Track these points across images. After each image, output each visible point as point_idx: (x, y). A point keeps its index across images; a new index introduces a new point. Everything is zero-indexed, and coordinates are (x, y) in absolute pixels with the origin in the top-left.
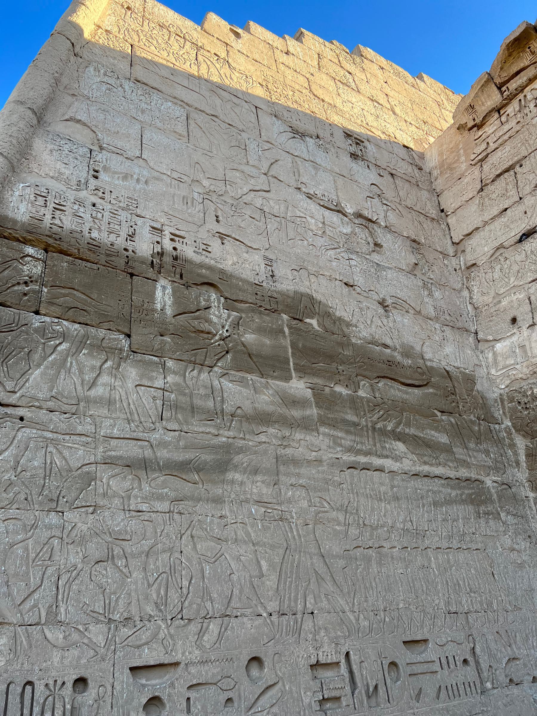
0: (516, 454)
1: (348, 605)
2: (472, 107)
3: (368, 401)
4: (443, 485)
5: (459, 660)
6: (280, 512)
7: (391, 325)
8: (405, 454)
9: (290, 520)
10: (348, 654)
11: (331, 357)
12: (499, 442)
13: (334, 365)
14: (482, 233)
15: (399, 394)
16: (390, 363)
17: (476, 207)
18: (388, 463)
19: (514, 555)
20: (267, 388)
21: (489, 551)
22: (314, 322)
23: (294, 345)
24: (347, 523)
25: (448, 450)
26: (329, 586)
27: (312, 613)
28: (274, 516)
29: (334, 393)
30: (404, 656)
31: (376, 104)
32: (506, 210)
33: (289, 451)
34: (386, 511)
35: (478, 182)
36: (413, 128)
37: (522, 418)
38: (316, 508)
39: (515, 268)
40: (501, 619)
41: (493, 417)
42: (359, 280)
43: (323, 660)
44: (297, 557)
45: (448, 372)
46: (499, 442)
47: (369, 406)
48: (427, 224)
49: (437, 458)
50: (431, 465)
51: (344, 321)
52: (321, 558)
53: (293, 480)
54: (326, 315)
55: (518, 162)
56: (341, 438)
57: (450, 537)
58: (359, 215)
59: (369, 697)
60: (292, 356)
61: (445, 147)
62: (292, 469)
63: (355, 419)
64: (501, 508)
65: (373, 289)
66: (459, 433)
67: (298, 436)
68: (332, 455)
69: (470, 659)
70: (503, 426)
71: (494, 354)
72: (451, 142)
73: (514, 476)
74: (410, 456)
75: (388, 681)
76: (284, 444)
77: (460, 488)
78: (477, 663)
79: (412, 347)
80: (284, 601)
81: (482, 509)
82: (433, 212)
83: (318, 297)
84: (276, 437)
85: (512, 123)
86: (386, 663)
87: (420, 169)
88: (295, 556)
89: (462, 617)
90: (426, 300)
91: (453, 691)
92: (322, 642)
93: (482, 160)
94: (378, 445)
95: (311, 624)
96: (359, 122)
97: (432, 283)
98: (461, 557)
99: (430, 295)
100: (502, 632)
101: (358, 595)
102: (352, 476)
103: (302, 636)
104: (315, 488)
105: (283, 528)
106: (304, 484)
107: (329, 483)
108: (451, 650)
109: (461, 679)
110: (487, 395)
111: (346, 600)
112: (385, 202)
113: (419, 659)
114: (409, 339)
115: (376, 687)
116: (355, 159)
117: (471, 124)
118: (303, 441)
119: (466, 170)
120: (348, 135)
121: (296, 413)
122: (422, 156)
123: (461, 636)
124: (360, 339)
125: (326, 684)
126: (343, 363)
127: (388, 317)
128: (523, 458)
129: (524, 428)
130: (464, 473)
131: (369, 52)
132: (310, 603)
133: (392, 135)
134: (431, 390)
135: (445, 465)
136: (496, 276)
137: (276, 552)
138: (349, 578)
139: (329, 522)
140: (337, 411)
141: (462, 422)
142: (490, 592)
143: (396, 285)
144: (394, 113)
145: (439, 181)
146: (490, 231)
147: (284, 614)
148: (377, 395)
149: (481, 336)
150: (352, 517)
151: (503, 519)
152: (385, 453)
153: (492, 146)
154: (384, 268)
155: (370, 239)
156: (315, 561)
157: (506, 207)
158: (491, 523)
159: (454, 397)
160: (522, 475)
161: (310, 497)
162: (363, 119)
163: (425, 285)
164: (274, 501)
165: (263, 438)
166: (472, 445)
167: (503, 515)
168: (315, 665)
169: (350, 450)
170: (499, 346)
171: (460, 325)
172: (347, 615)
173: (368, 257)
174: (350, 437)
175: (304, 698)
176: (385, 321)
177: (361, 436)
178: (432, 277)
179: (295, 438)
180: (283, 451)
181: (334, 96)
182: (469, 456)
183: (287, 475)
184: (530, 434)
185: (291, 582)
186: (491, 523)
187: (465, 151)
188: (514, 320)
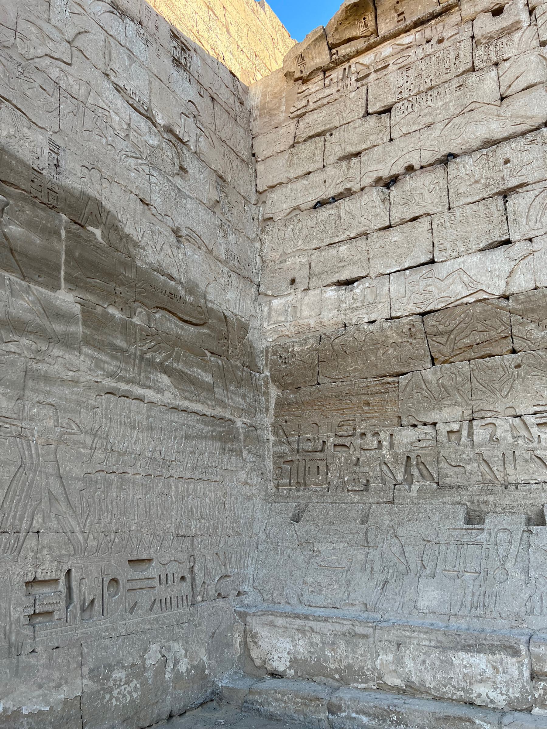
0: (267, 401)
1: (79, 526)
2: (302, 57)
3: (142, 329)
4: (197, 421)
5: (178, 576)
6: (20, 429)
7: (181, 257)
8: (168, 387)
9: (30, 438)
10: (69, 571)
11: (109, 275)
12: (256, 389)
13: (112, 285)
14: (284, 190)
15: (174, 328)
16: (172, 295)
17: (285, 161)
18: (149, 394)
19: (245, 489)
20: (28, 293)
21: (226, 483)
22: (98, 232)
23: (69, 252)
24: (94, 446)
25: (210, 389)
26: (63, 507)
27: (38, 532)
28: (11, 432)
29: (106, 315)
30: (126, 574)
31: (211, 13)
32: (310, 173)
33: (41, 367)
34: (137, 439)
35: (292, 137)
36: (243, 57)
37: (279, 371)
38: (62, 429)
39: (305, 232)
40: (222, 543)
41: (256, 365)
42: (157, 200)
43: (40, 577)
44: (31, 475)
46: (256, 389)
47: (141, 334)
48: (236, 164)
49: (198, 395)
50: (191, 401)
51: (132, 240)
52: (59, 480)
53: (41, 398)
54: (113, 228)
55: (330, 130)
56: (105, 362)
57: (194, 469)
58: (170, 131)
59: (83, 610)
60: (65, 264)
61: (269, 89)
62: (42, 385)
63: (124, 345)
64: (245, 446)
65: (169, 214)
66: (224, 375)
67: (56, 352)
68: (91, 378)
69: (188, 576)
70: (263, 375)
72: (276, 86)
73: (261, 420)
74: (173, 390)
75: (106, 596)
76: (38, 358)
77: (212, 425)
78: (193, 579)
79: (197, 285)
80: (7, 519)
81: (228, 446)
82: (245, 154)
83: (109, 206)
84: (29, 349)
85: (333, 90)
86: (107, 579)
87: (242, 103)
88: (29, 474)
89: (188, 540)
90: (220, 241)
91: (165, 604)
92: (43, 560)
93: (300, 116)
94: (143, 375)
95: (34, 542)
96: (189, 25)
97: (229, 226)
98: (200, 487)
99: (225, 237)
100: (221, 554)
101: (91, 517)
102: (109, 401)
103: (21, 554)
104: (65, 409)
105: (20, 445)
106: (53, 403)
107: (83, 405)
108: (172, 568)
109: (176, 593)
110: (255, 345)
111: (78, 521)
112: (199, 125)
113: (140, 576)
114: (196, 276)
115: (92, 602)
117: (297, 75)
118: (60, 359)
119: (284, 121)
120: (175, 36)
121: (58, 328)
122: (246, 91)
123: (183, 556)
124: (146, 264)
125: (39, 600)
126: (122, 284)
127: (179, 248)
128: (272, 405)
130: (219, 412)
132: (38, 522)
133: (221, 55)
134: (206, 331)
135: (204, 403)
136: (287, 236)
137: (6, 470)
138: (85, 500)
139: (75, 444)
140: (105, 333)
141: (228, 366)
142: (218, 519)
143: (193, 217)
144: (228, 32)
145: (257, 123)
146: (292, 189)
147: (4, 532)
148: (152, 325)
150: (100, 442)
151: (244, 456)
152: (148, 383)
153: (312, 106)
154: (185, 196)
155: (176, 160)
156: (51, 481)
157: (310, 170)
158: (233, 459)
159: (226, 341)
160: (268, 420)
161: (58, 417)
162: (195, 24)
163: (222, 225)
164: (15, 416)
165: (12, 347)
166: (232, 388)
167: (244, 453)
168: (32, 582)
169: (112, 375)
170: (275, 302)
171: (246, 274)
172: (76, 535)
173: (170, 178)
174: (115, 363)
175: (12, 614)
176: (175, 251)
177: (127, 363)
178: (230, 219)
179: (52, 354)
180: (34, 366)
182: (228, 397)
183: (36, 391)
184: (282, 386)
185: (19, 501)
186: (233, 459)
187: (287, 101)
188: (293, 281)
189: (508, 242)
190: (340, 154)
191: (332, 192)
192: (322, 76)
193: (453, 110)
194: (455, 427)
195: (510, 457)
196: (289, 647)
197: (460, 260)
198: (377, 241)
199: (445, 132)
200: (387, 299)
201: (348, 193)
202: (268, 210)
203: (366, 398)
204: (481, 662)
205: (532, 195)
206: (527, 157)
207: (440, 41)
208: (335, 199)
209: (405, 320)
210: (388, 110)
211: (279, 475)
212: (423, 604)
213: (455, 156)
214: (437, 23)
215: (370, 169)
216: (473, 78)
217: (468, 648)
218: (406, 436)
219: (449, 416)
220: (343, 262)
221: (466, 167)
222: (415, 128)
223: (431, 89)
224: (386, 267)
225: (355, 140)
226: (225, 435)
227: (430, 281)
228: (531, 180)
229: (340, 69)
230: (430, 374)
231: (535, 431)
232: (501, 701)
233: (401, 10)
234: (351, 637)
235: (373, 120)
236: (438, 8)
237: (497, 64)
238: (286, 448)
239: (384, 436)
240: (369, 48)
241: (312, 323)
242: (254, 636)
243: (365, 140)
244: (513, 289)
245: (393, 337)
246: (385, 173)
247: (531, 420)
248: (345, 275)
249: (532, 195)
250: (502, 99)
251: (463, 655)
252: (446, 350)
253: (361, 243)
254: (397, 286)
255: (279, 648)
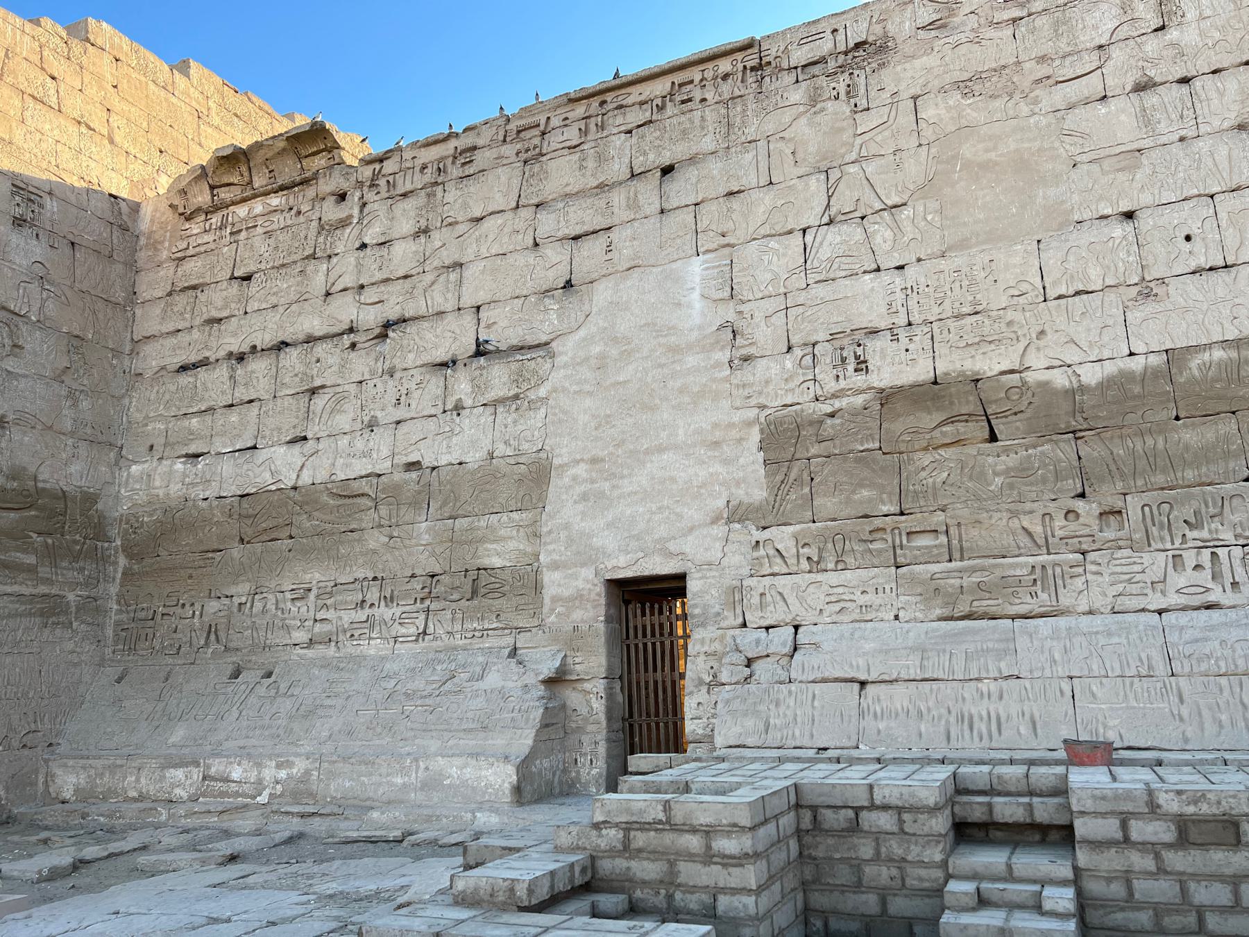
0: (115, 571)
4: (12, 602)
25: (31, 570)
35: (170, 282)
39: (167, 397)
45: (64, 492)
55: (203, 285)
71: (129, 474)
79: (25, 469)
85: (208, 238)
97: (82, 391)
99: (75, 405)
110: (107, 514)
114: (24, 459)
116: (19, 225)
117: (181, 210)
129: (127, 550)
130: (43, 589)
131: (103, 31)
133: (95, 181)
135: (21, 584)
144: (111, 141)
149: (124, 453)
153: (191, 251)
154: (16, 376)
160: (114, 589)
162: (53, 160)
178: (85, 382)
181: (14, 124)
182: (57, 574)
184: (130, 556)
188: (152, 447)
189: (305, 438)
190: (205, 317)
191: (193, 358)
192: (203, 217)
193: (293, 297)
194: (243, 599)
195: (270, 627)
196: (75, 780)
197: (273, 449)
198: (220, 419)
199: (284, 318)
200: (218, 478)
201: (204, 363)
202: (138, 365)
203: (190, 571)
204: (179, 774)
205: (327, 397)
206: (330, 361)
207: (299, 213)
208: (195, 366)
209: (228, 501)
210: (248, 278)
211: (116, 643)
212: (170, 741)
213: (287, 344)
214: (300, 191)
215: (226, 341)
216: (311, 266)
217: (175, 766)
218: (213, 606)
219: (241, 590)
220: (192, 435)
221: (292, 357)
222: (264, 306)
223: (283, 265)
224: (225, 447)
225: (220, 304)
226: (51, 611)
227: (250, 466)
228: (328, 384)
229: (219, 214)
230: (236, 552)
231: (289, 604)
232: (184, 795)
233: (271, 168)
234: (113, 769)
235: (235, 284)
236: (298, 179)
237: (330, 257)
238: (124, 617)
239: (198, 606)
240: (244, 200)
241: (161, 494)
242: (53, 776)
243: (226, 306)
244: (300, 483)
245: (218, 516)
246: (235, 348)
247: (289, 596)
248: (193, 449)
249: (327, 397)
250: (328, 294)
251: (172, 770)
252: (250, 531)
253: (208, 418)
254: (227, 468)
255: (68, 782)
